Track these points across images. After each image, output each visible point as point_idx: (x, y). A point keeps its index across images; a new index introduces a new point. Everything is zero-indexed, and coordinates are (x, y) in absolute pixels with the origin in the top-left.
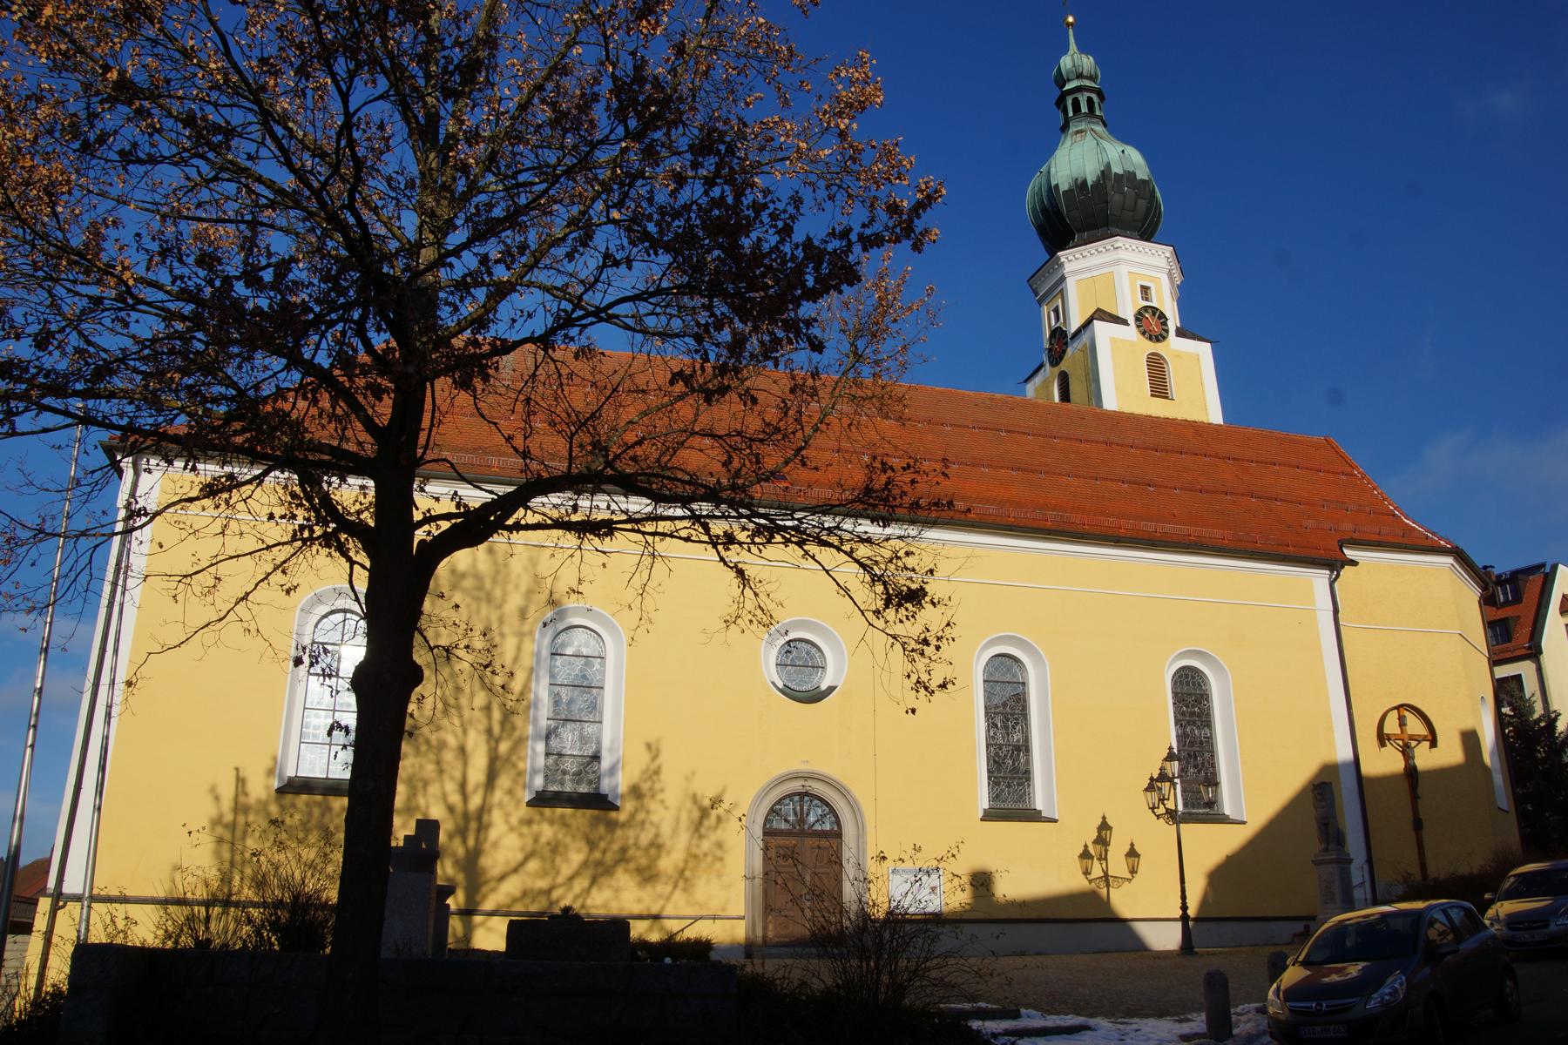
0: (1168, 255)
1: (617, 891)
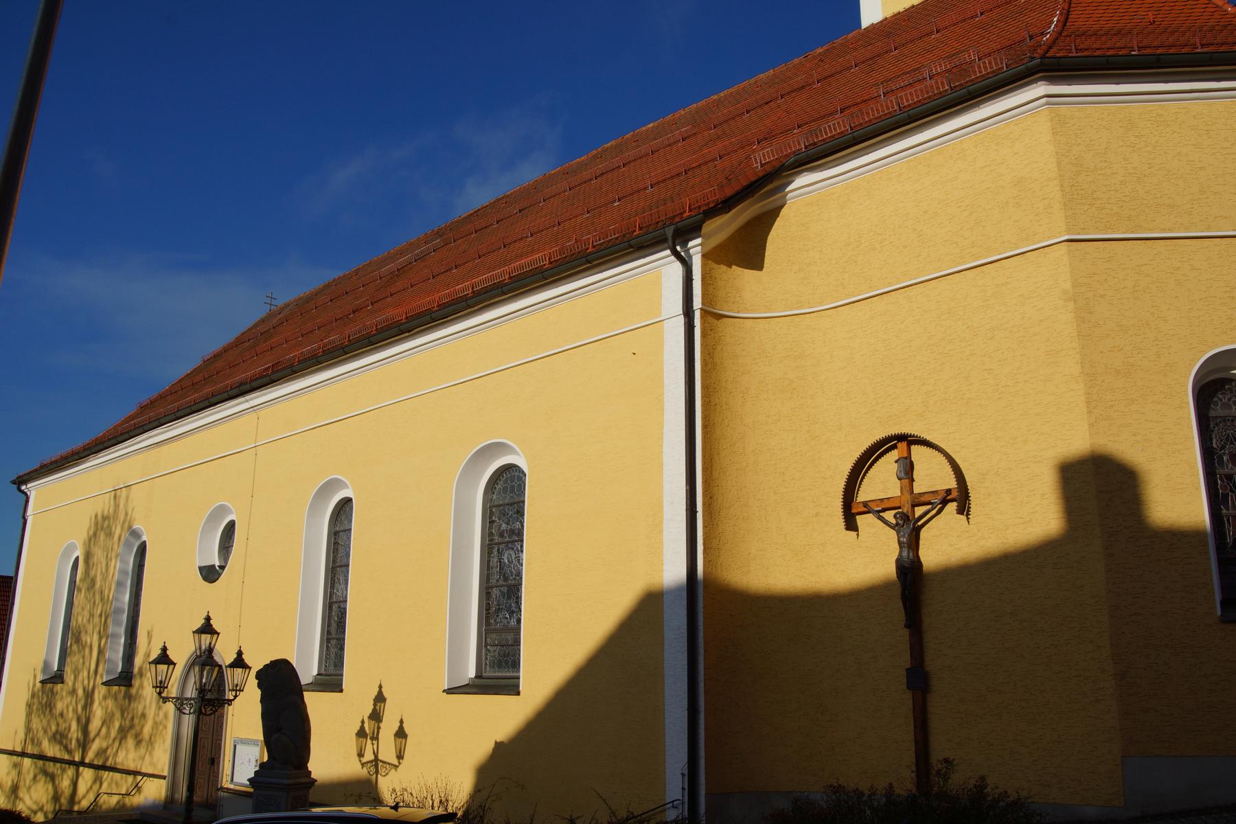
1: (127, 751)
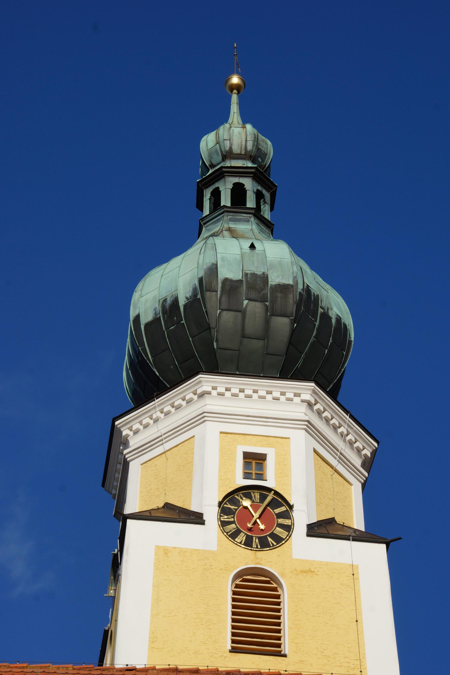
0: (307, 396)
